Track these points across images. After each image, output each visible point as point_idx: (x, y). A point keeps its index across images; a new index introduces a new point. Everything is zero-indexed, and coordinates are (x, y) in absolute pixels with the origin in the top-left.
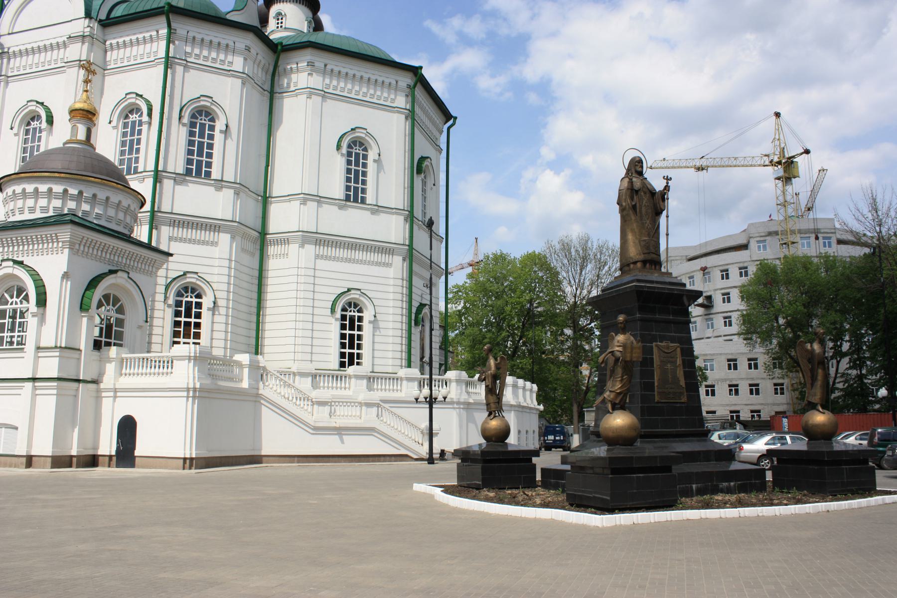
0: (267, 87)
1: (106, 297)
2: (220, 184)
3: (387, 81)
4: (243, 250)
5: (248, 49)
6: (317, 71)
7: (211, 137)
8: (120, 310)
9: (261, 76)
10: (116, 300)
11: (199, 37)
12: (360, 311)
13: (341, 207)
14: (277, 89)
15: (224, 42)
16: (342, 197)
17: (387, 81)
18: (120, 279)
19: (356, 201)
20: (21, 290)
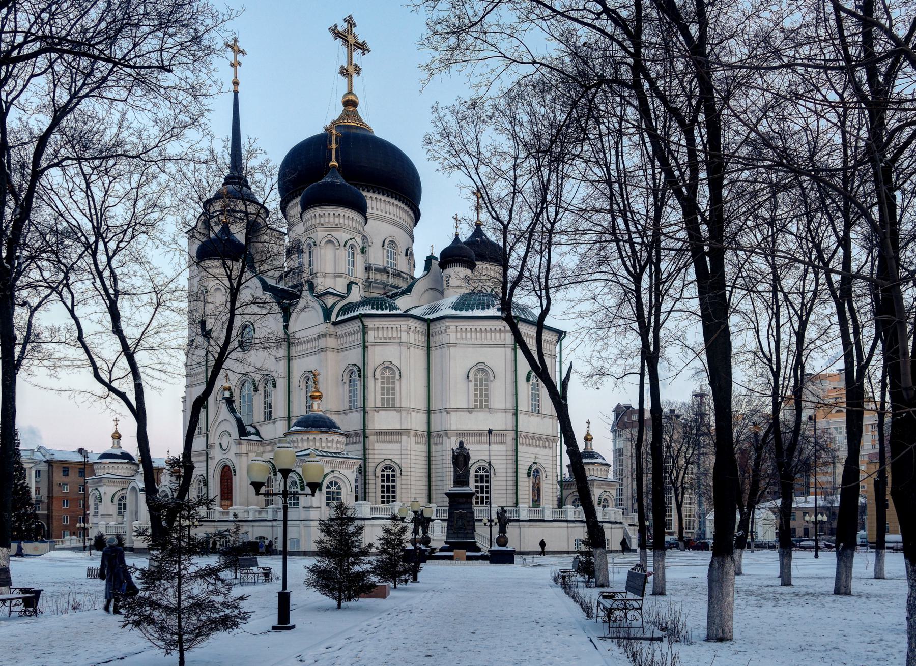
0: (426, 345)
1: (331, 483)
2: (399, 410)
3: (498, 328)
4: (417, 443)
5: (409, 328)
6: (452, 331)
7: (393, 383)
8: (339, 487)
9: (422, 339)
10: (336, 483)
11: (380, 327)
12: (487, 472)
13: (470, 413)
14: (432, 344)
15: (394, 327)
16: (472, 406)
17: (498, 328)
18: (336, 474)
19: (481, 407)
20: (296, 483)
